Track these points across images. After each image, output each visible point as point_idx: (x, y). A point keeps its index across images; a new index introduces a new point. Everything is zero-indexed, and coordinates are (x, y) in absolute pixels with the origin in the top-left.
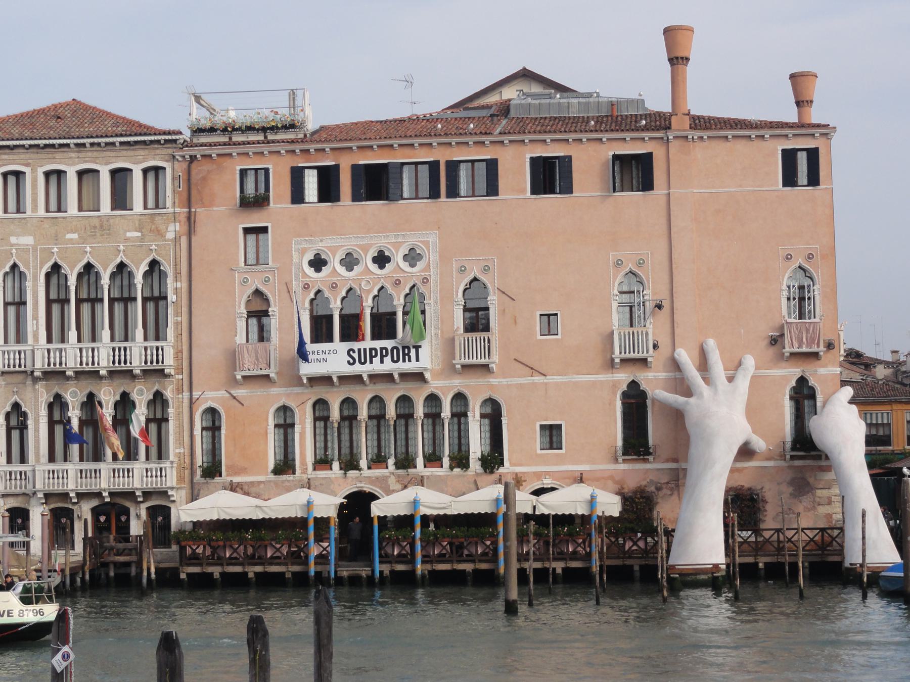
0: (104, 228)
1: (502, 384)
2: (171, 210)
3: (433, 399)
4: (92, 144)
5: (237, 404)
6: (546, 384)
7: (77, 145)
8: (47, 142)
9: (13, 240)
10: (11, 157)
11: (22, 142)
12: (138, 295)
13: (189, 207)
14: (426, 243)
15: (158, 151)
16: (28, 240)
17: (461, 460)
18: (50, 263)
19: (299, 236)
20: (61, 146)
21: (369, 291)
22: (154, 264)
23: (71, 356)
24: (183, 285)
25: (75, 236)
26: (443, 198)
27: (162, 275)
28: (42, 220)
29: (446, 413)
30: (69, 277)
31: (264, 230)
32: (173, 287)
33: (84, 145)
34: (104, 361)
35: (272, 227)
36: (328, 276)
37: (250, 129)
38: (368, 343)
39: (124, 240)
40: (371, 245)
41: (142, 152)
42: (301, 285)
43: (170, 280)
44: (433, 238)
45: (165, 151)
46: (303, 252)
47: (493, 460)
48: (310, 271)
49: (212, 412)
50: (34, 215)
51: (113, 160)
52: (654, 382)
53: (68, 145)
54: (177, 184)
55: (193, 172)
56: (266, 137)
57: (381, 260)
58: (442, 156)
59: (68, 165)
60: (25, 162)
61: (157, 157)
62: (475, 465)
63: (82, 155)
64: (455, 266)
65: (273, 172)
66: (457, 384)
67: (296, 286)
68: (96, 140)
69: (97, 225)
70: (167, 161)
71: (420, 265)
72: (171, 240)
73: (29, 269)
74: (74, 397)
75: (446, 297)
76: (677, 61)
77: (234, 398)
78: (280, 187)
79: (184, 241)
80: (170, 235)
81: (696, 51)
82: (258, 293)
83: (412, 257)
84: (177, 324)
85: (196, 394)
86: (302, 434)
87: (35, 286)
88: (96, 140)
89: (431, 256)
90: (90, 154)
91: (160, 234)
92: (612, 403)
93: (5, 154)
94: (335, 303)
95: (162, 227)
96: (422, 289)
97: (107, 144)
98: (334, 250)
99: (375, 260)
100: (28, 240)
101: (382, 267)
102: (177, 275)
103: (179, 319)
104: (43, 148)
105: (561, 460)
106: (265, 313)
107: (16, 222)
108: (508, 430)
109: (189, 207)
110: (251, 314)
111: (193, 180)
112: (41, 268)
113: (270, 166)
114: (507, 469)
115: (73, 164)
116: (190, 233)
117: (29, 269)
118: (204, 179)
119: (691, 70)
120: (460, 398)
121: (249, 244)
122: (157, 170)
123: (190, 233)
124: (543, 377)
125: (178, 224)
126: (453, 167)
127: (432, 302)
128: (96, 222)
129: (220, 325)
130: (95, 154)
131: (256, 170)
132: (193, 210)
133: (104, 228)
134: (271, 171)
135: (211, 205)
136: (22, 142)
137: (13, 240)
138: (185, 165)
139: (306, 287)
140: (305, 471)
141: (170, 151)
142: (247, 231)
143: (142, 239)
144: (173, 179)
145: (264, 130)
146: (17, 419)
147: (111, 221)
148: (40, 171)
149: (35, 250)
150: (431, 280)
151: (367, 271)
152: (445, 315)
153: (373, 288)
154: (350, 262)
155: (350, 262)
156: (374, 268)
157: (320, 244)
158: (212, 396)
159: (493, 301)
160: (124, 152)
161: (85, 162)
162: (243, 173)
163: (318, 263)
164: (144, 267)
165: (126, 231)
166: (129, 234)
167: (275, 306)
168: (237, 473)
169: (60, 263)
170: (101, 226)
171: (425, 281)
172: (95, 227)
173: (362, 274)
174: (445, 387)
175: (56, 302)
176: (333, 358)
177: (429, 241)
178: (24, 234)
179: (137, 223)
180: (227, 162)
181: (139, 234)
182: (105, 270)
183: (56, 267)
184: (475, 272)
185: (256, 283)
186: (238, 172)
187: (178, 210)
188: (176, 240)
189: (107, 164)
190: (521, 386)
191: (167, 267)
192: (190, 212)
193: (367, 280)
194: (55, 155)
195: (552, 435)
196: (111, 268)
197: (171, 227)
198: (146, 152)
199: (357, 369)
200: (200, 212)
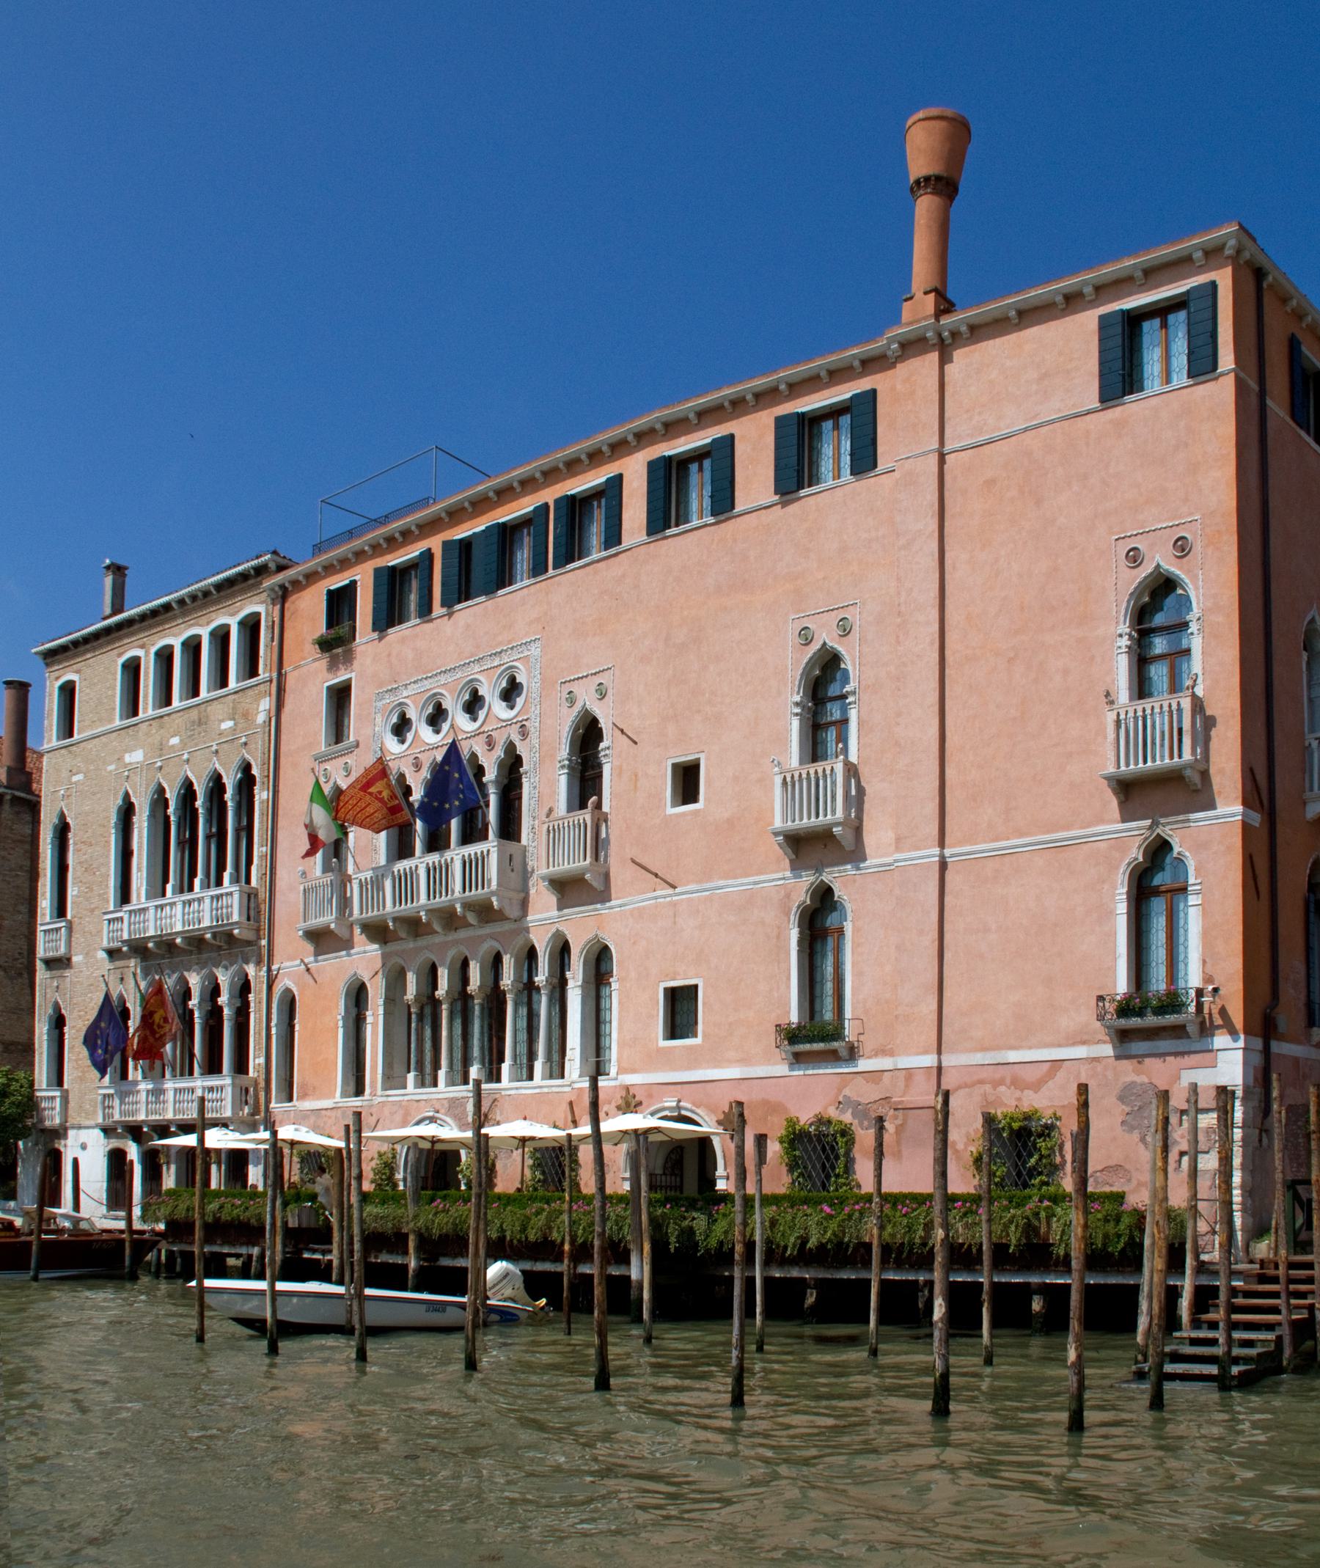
5: (311, 981)
6: (674, 904)
25: (175, 741)
48: (393, 745)
60: (140, 642)
77: (308, 970)
80: (261, 718)
83: (511, 692)
84: (261, 857)
85: (274, 967)
86: (375, 1025)
92: (781, 937)
108: (620, 1003)
124: (670, 891)
137: (128, 758)
140: (373, 1094)
143: (234, 730)
152: (546, 787)
154: (437, 717)
161: (192, 625)
163: (401, 727)
171: (524, 733)
190: (639, 914)
191: (255, 771)
197: (261, 708)
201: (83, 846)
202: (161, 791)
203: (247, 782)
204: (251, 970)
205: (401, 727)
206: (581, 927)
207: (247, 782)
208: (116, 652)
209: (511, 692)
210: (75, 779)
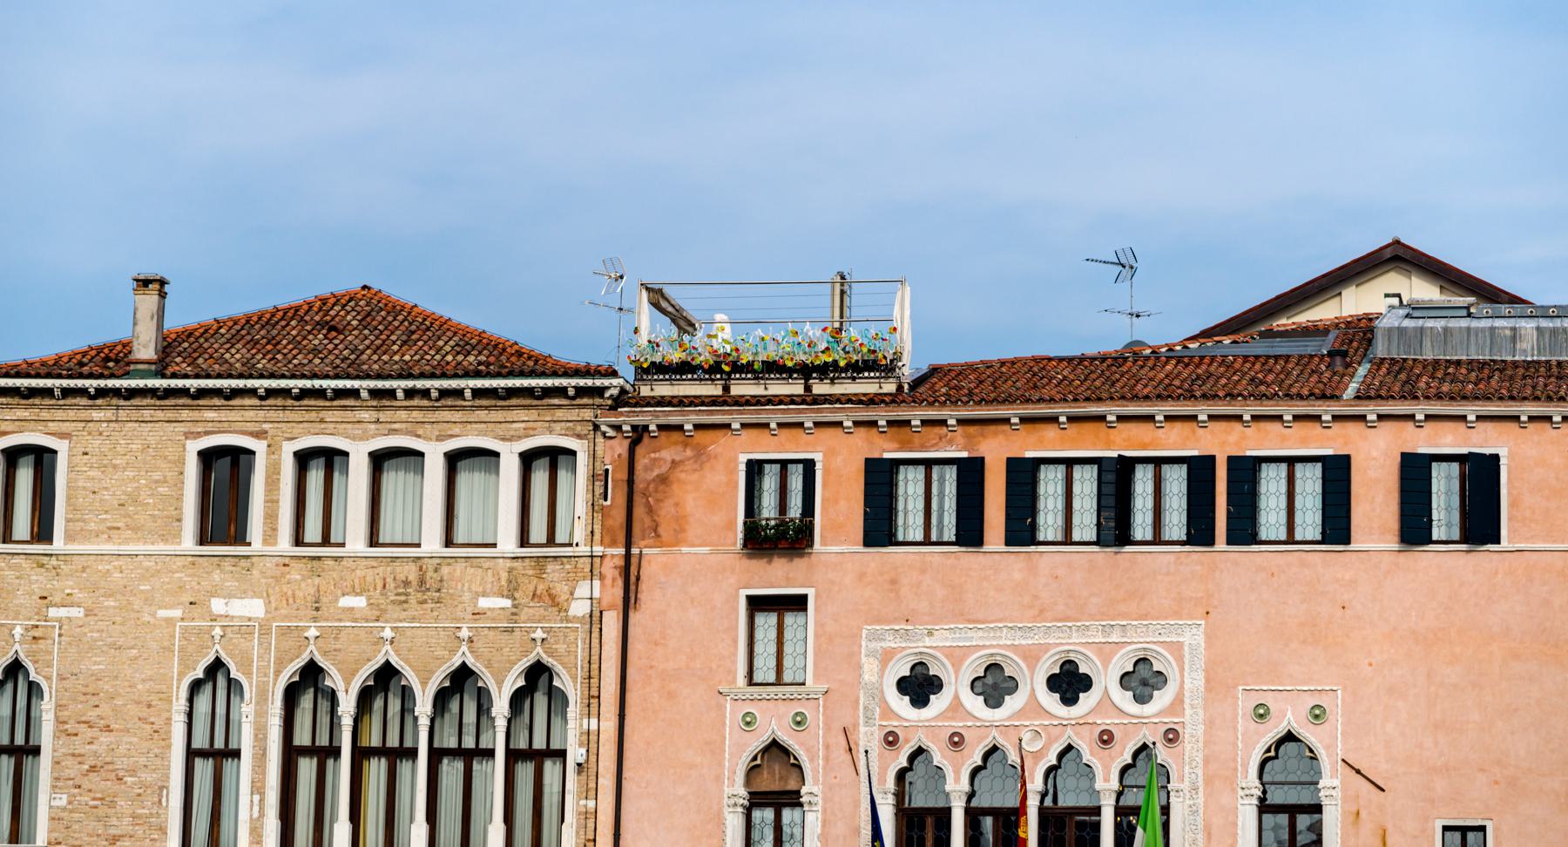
0: (425, 586)
2: (584, 549)
4: (410, 393)
7: (374, 393)
8: (308, 384)
9: (218, 606)
10: (224, 415)
11: (251, 383)
13: (628, 546)
14: (1176, 648)
15: (560, 414)
16: (253, 608)
18: (300, 663)
19: (879, 621)
20: (340, 393)
21: (1038, 755)
22: (538, 674)
25: (359, 602)
26: (1221, 543)
27: (557, 699)
28: (286, 562)
30: (341, 695)
31: (798, 603)
33: (391, 394)
35: (817, 596)
36: (942, 716)
37: (773, 368)
40: (1047, 647)
41: (522, 415)
42: (878, 736)
43: (573, 711)
44: (1193, 637)
45: (573, 414)
46: (886, 657)
48: (902, 705)
50: (269, 550)
51: (456, 429)
53: (354, 393)
54: (599, 490)
55: (642, 462)
56: (808, 388)
57: (1069, 683)
58: (1222, 443)
59: (354, 439)
61: (557, 427)
63: (384, 416)
64: (1245, 704)
65: (826, 471)
67: (869, 737)
68: (420, 384)
69: (413, 577)
70: (579, 436)
71: (1162, 699)
72: (580, 620)
73: (248, 674)
75: (1218, 777)
78: (839, 507)
79: (612, 622)
80: (580, 608)
82: (775, 749)
83: (1142, 679)
87: (261, 714)
88: (420, 384)
89: (1186, 679)
90: (403, 415)
91: (554, 602)
93: (211, 408)
94: (957, 780)
95: (561, 589)
96: (1162, 754)
97: (444, 393)
98: (957, 656)
99: (1053, 683)
100: (253, 608)
101: (1069, 700)
102: (592, 700)
103: (591, 804)
104: (299, 397)
106: (792, 799)
107: (227, 564)
109: (628, 546)
110: (757, 800)
111: (639, 485)
112: (278, 673)
113: (818, 457)
115: (364, 437)
116: (628, 603)
117: (248, 674)
118: (663, 480)
121: (759, 634)
122: (555, 457)
123: (628, 603)
125: (597, 583)
126: (1246, 471)
127: (1186, 785)
128: (411, 572)
130: (417, 415)
131: (784, 464)
132: (635, 551)
133: (425, 586)
134: (819, 466)
135: (677, 542)
136: (251, 383)
137: (218, 606)
138: (620, 447)
139: (891, 740)
141: (588, 414)
142: (757, 604)
144: (593, 477)
145: (805, 371)
147: (445, 570)
148: (288, 450)
149: (265, 630)
150: (1186, 734)
151: (1034, 707)
153: (1046, 748)
154: (994, 684)
155: (994, 684)
156: (1051, 701)
157: (928, 641)
159: (1332, 787)
160: (482, 415)
162: (755, 469)
163: (919, 686)
164: (514, 680)
165: (477, 595)
166: (484, 603)
167: (816, 782)
169: (321, 661)
170: (422, 582)
171: (1172, 737)
172: (407, 583)
173: (1020, 713)
177: (1185, 649)
178: (243, 594)
179: (504, 575)
180: (719, 444)
181: (507, 603)
182: (424, 684)
183: (312, 673)
184: (1290, 717)
185: (774, 724)
186: (743, 467)
187: (598, 550)
188: (595, 620)
189: (440, 438)
191: (566, 681)
192: (628, 556)
194: (323, 414)
196: (438, 679)
197: (583, 590)
198: (533, 414)
200: (653, 558)
201: (90, 733)
202: (312, 673)
205: (920, 686)
208: (181, 428)
209: (1142, 679)
210: (52, 612)
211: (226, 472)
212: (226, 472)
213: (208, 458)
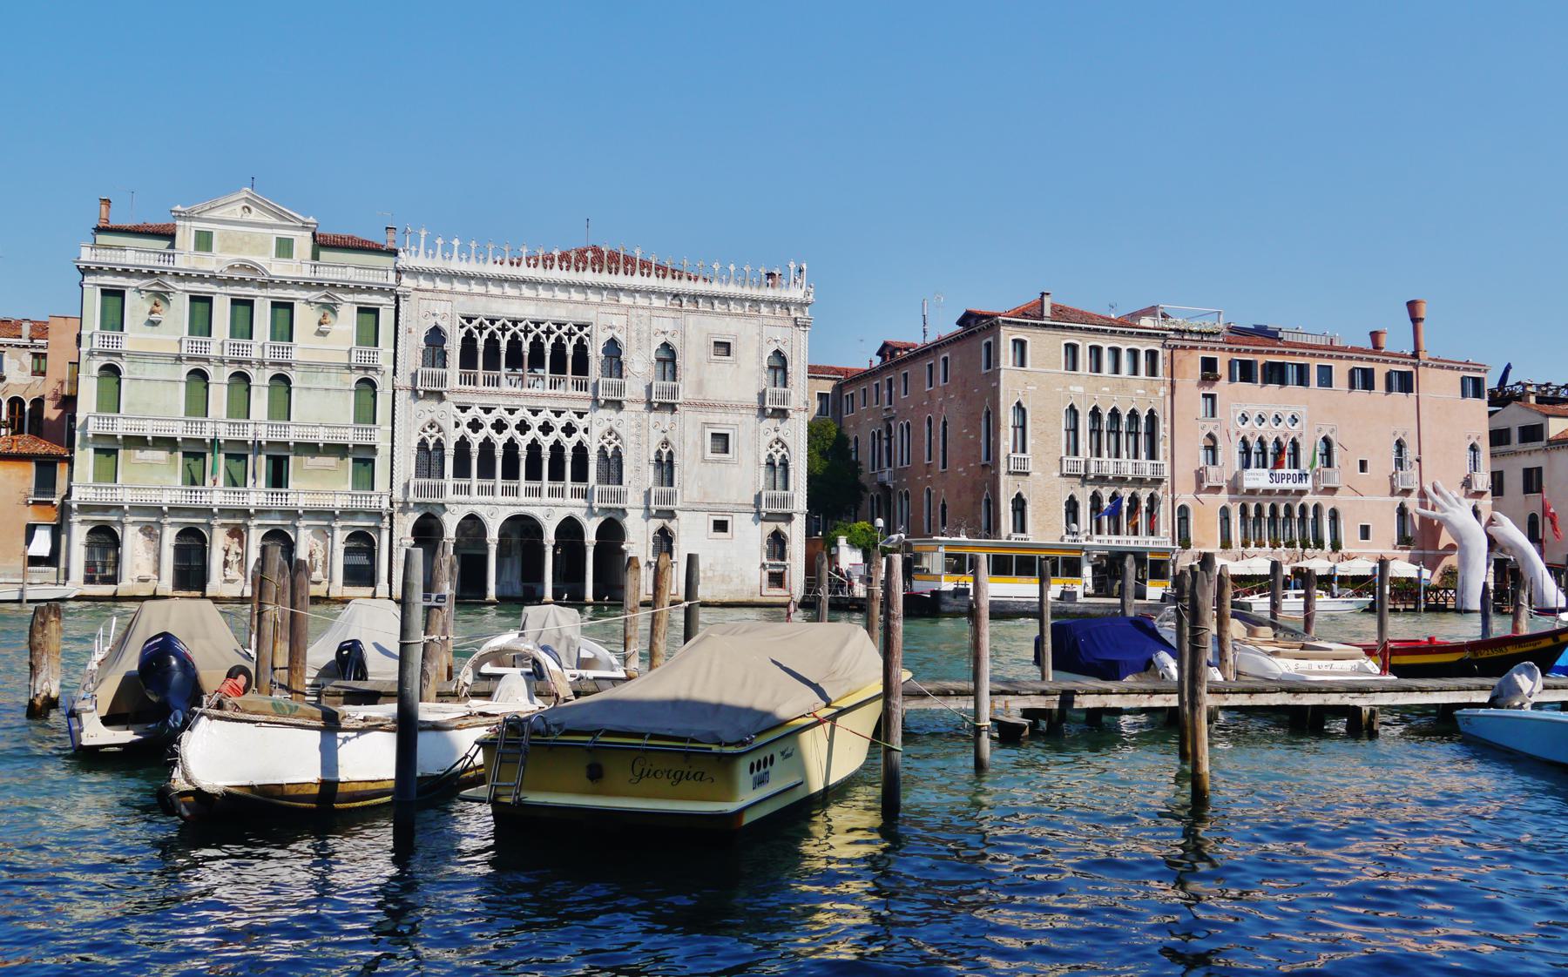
0: (1124, 385)
1: (1339, 501)
3: (1303, 508)
12: (1144, 431)
16: (1080, 389)
17: (1319, 544)
22: (1151, 412)
23: (1108, 466)
24: (1168, 426)
29: (1311, 516)
32: (1163, 428)
34: (1129, 473)
38: (1286, 471)
39: (1131, 393)
47: (1336, 546)
49: (1184, 510)
52: (1412, 503)
62: (1328, 548)
66: (1318, 498)
67: (1233, 435)
74: (1106, 493)
76: (1416, 320)
81: (1423, 312)
82: (1210, 436)
83: (1294, 420)
89: (1303, 420)
100: (1080, 389)
105: (1369, 546)
110: (1206, 448)
114: (1344, 550)
119: (1422, 326)
120: (1317, 507)
129: (1190, 456)
142: (1205, 396)
146: (1072, 507)
158: (1185, 497)
159: (1336, 448)
163: (1245, 418)
168: (1202, 545)
174: (1310, 500)
175: (1096, 431)
176: (1258, 478)
183: (1095, 409)
185: (1209, 429)
191: (1159, 414)
193: (1270, 432)
195: (1365, 532)
199: (1274, 486)
202: (1095, 409)
203: (1152, 416)
204: (1159, 493)
205: (1245, 418)
206: (1328, 503)
207: (1152, 416)
211: (1072, 349)
212: (1072, 349)
213: (1067, 345)
